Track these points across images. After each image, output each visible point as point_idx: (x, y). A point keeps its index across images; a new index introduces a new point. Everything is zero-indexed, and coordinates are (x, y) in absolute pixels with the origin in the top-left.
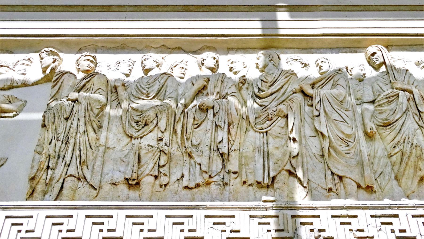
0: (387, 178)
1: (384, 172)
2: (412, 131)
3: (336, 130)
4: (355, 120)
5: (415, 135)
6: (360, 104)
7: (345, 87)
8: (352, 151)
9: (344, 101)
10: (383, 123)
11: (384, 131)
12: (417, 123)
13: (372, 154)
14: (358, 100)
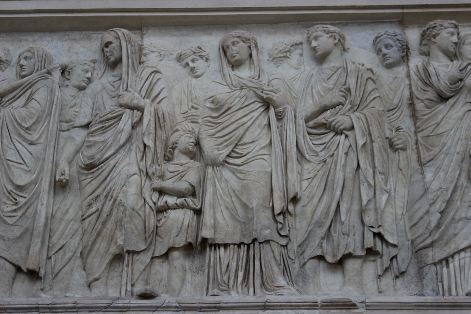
0: (68, 255)
1: (67, 245)
2: (122, 178)
3: (4, 178)
4: (44, 160)
5: (124, 185)
6: (68, 130)
7: (43, 102)
8: (19, 213)
9: (33, 128)
10: (84, 164)
11: (84, 177)
12: (138, 163)
13: (59, 215)
14: (67, 122)
